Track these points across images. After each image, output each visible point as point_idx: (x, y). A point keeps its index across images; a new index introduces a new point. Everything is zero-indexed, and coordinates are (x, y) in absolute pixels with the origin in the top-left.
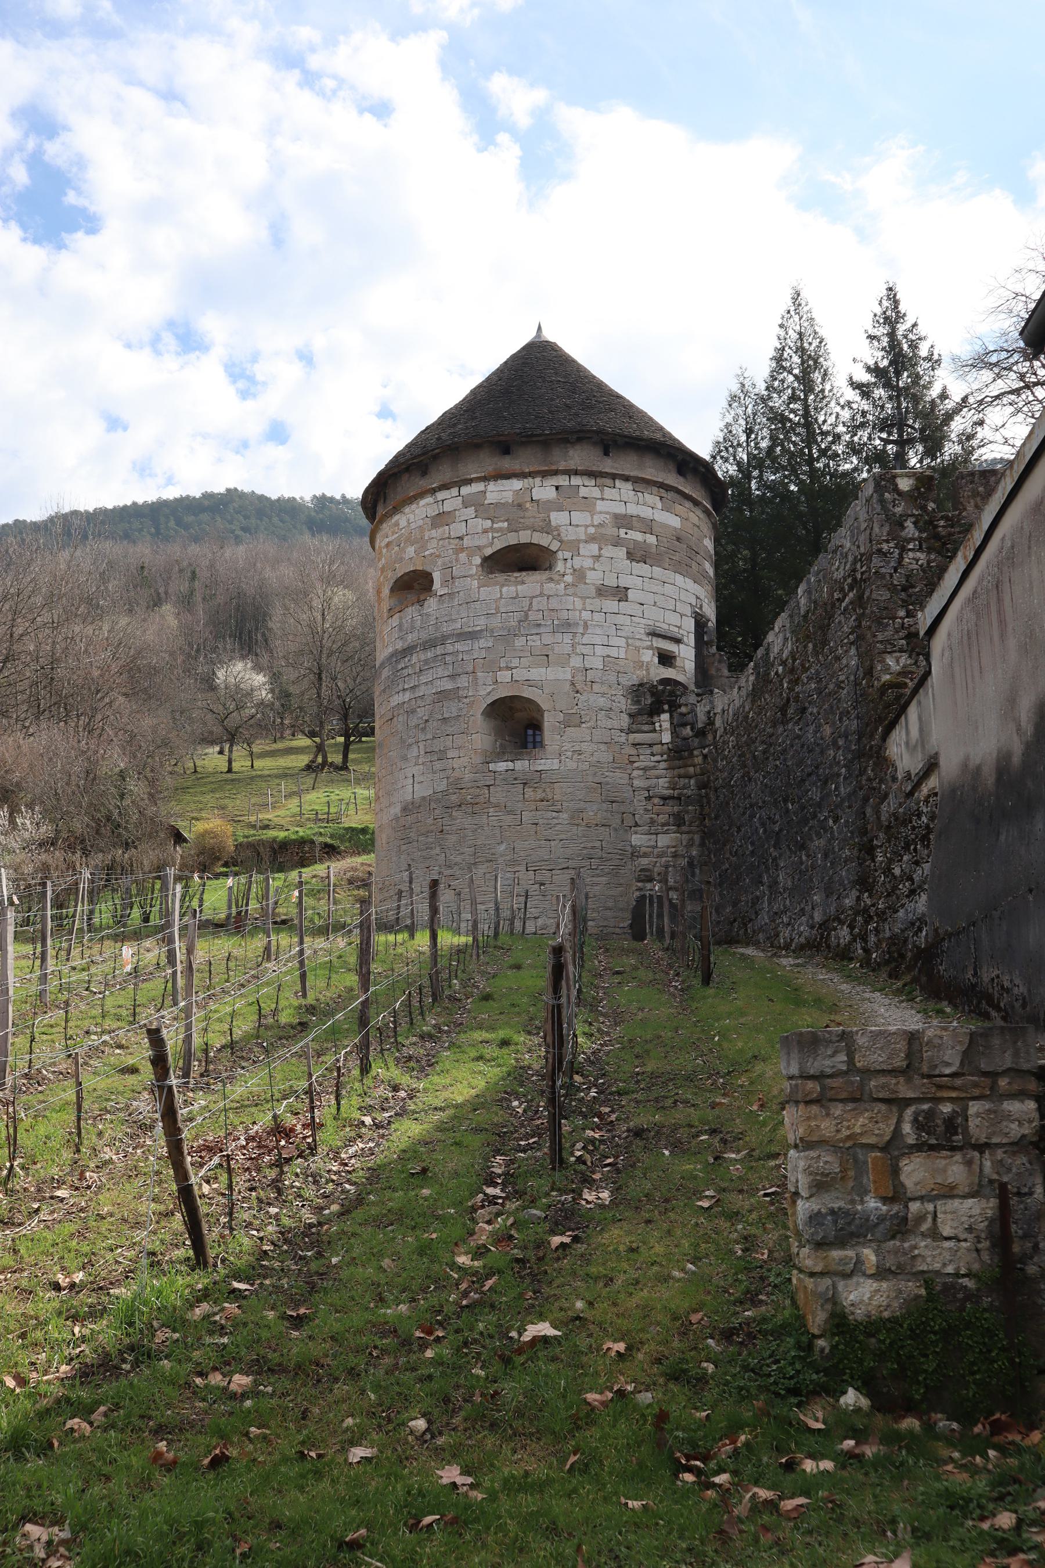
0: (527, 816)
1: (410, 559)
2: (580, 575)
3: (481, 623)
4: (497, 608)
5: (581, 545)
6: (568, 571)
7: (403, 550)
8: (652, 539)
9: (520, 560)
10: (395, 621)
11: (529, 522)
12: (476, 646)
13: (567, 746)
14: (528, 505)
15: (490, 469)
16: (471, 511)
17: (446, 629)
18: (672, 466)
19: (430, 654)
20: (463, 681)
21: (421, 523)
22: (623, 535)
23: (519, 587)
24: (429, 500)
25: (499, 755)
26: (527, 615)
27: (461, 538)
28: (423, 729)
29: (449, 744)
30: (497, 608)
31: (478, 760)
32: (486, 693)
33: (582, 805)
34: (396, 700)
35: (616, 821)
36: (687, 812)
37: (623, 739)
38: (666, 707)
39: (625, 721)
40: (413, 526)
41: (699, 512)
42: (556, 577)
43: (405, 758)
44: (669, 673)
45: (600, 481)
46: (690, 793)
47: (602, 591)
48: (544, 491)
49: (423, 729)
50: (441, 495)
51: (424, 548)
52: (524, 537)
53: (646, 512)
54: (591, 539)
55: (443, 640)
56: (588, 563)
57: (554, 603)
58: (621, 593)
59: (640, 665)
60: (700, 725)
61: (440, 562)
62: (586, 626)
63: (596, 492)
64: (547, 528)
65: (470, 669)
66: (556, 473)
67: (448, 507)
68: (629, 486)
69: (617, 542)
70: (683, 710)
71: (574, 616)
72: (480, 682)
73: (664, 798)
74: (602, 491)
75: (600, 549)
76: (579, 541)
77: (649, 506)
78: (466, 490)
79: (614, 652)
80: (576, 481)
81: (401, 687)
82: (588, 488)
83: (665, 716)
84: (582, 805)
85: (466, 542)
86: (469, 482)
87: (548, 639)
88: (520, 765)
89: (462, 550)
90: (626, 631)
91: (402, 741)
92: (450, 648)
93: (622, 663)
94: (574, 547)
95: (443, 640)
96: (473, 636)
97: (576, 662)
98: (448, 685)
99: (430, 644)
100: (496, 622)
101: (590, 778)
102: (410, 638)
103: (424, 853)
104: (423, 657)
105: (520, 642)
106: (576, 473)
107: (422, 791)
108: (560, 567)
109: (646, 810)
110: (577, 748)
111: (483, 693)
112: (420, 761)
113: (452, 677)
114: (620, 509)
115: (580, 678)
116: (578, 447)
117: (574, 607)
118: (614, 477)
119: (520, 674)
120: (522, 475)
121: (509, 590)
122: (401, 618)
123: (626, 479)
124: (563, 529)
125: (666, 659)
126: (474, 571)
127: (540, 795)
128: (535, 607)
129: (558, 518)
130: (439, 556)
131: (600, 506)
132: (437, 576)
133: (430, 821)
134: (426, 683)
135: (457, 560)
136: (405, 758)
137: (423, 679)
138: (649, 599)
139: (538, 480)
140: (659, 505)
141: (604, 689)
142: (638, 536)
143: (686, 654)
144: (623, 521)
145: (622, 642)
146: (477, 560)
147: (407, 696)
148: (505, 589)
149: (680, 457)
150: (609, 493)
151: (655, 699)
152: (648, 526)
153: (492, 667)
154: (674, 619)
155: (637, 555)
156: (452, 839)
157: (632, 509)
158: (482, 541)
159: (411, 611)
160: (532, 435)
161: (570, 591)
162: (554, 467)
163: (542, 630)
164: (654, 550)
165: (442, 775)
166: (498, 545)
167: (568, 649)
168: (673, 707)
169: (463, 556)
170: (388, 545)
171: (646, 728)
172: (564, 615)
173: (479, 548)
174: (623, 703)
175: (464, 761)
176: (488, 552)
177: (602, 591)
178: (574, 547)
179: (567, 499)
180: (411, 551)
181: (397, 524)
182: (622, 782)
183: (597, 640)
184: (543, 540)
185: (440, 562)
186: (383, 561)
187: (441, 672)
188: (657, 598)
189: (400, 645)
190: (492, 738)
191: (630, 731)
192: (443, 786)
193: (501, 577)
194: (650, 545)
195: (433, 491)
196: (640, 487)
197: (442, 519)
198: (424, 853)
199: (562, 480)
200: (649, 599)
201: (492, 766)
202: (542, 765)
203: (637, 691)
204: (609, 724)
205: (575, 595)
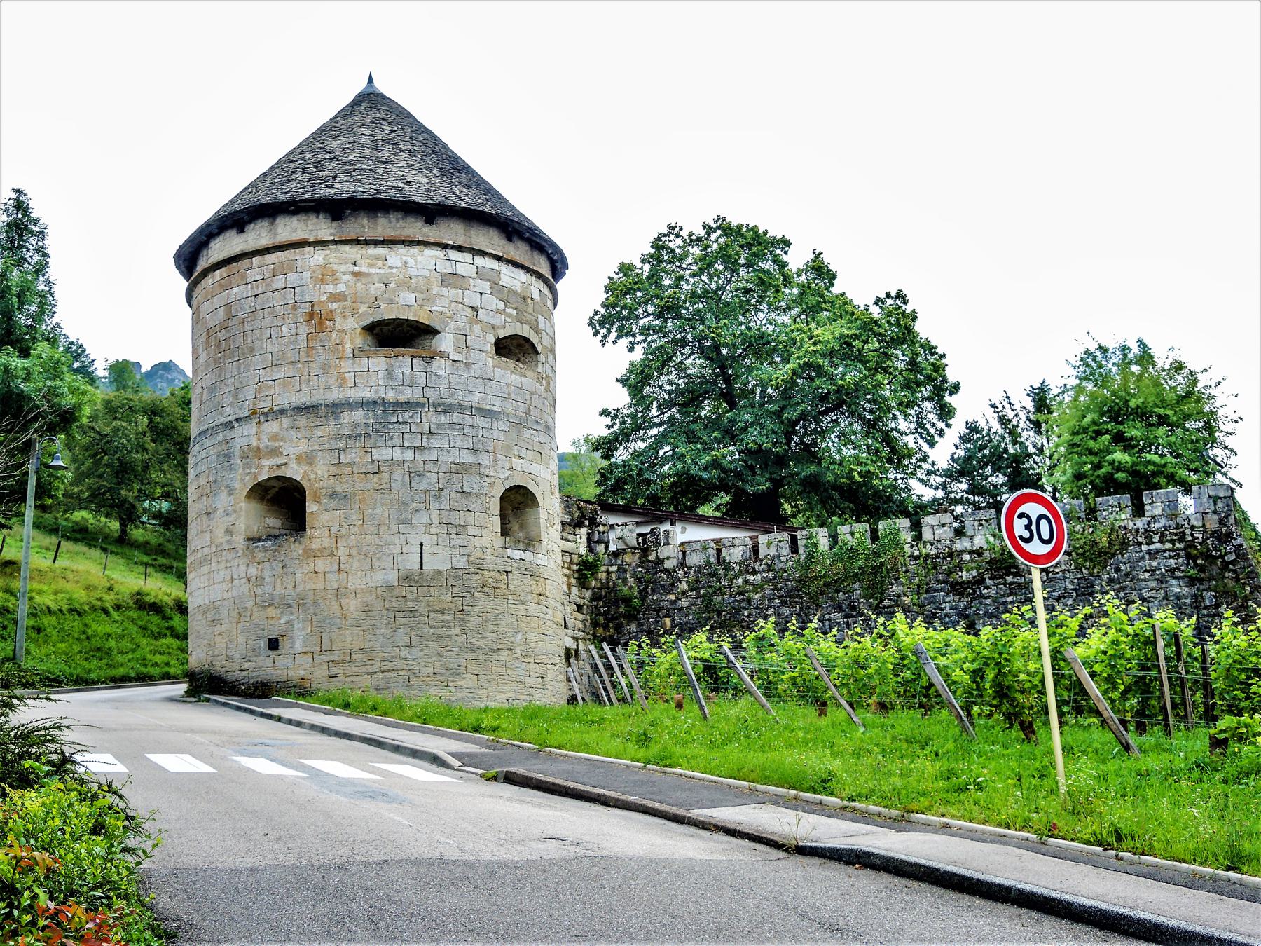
1: (405, 306)
3: (496, 405)
17: (460, 398)
19: (443, 419)
20: (484, 459)
21: (427, 273)
24: (438, 253)
28: (437, 498)
34: (385, 454)
38: (587, 522)
49: (437, 498)
50: (454, 255)
51: (433, 299)
55: (461, 409)
65: (491, 449)
67: (461, 269)
70: (601, 528)
72: (500, 465)
78: (479, 261)
86: (483, 254)
96: (491, 414)
98: (469, 459)
100: (509, 407)
103: (438, 632)
104: (434, 419)
112: (433, 530)
113: (474, 451)
133: (447, 598)
134: (442, 449)
136: (408, 522)
137: (435, 443)
147: (409, 455)
156: (475, 620)
158: (498, 320)
165: (463, 551)
169: (477, 328)
173: (494, 327)
176: (502, 334)
180: (409, 298)
184: (535, 340)
185: (452, 324)
187: (458, 441)
192: (463, 563)
195: (445, 247)
198: (438, 632)
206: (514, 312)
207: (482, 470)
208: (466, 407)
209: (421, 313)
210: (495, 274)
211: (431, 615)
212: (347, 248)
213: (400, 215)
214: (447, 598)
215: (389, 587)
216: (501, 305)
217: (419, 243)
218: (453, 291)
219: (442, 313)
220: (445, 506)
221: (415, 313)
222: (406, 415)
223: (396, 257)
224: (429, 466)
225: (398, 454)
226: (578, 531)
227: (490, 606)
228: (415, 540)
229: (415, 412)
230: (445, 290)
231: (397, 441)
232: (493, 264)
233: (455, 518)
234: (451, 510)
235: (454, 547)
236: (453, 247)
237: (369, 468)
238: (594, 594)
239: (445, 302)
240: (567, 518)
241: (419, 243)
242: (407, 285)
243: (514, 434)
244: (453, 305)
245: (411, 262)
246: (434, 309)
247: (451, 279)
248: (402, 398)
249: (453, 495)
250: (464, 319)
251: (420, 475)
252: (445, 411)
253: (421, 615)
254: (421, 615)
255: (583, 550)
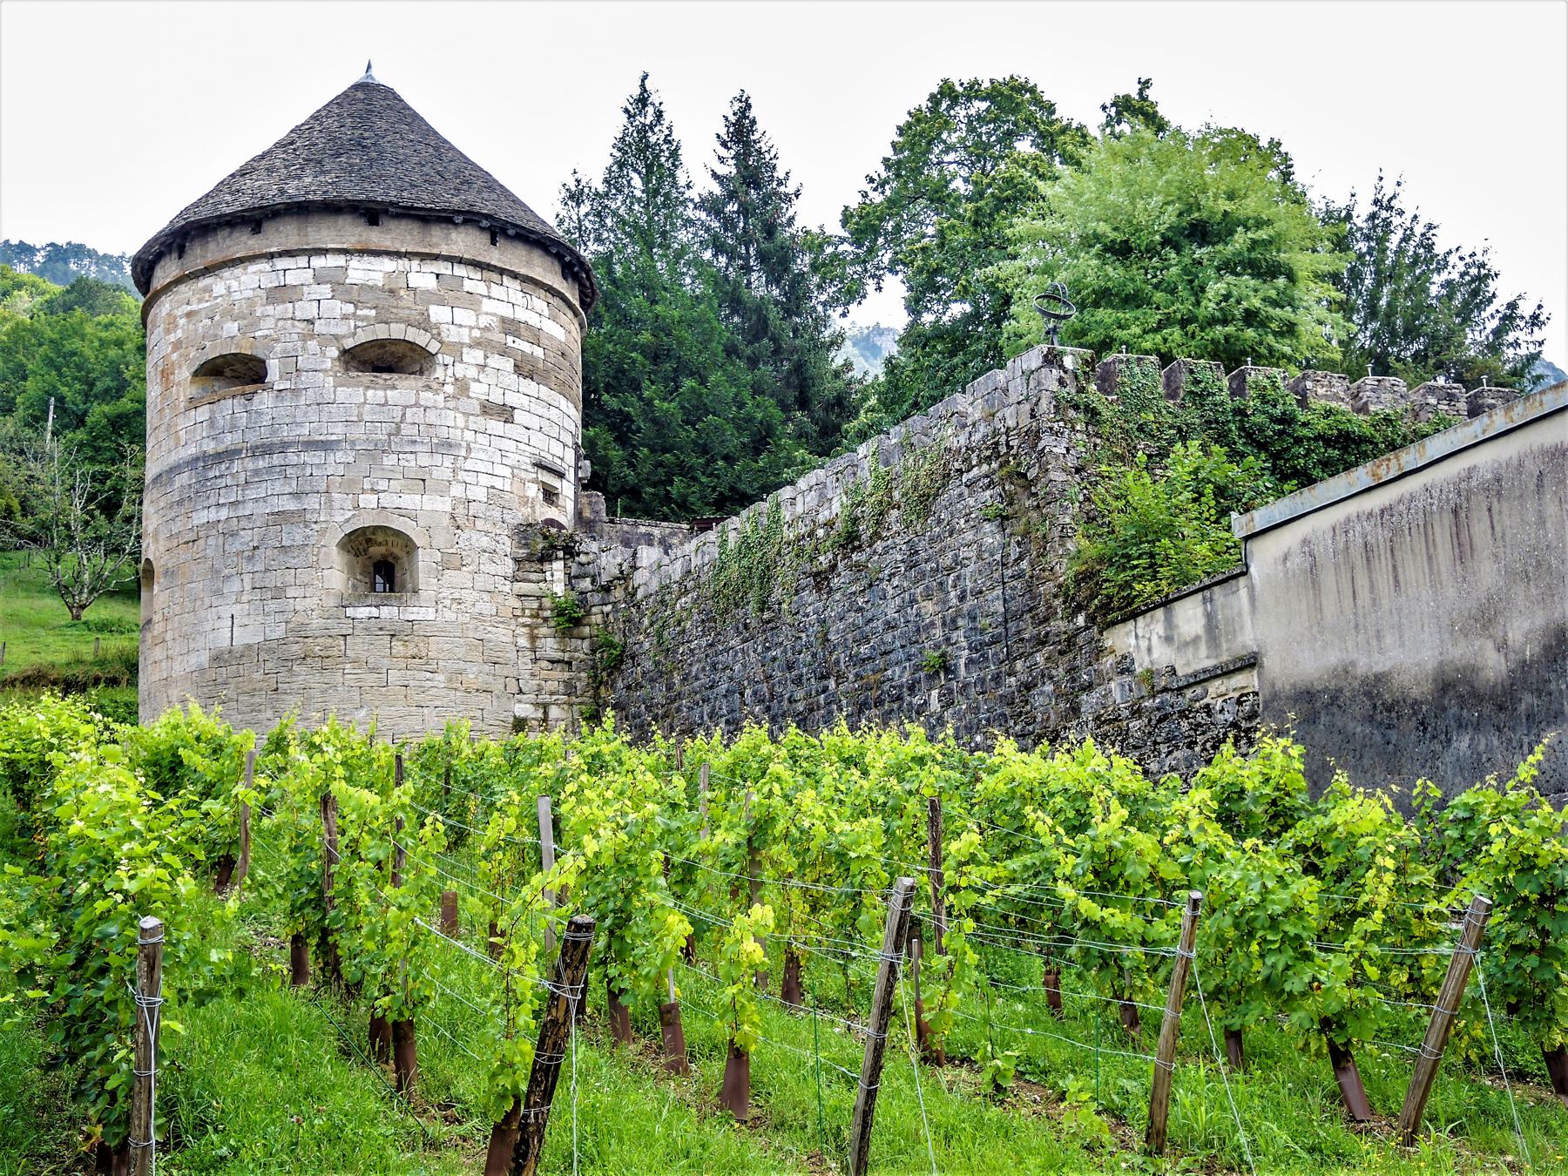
0: (394, 676)
1: (230, 338)
2: (462, 386)
3: (338, 432)
4: (360, 415)
5: (465, 350)
6: (449, 380)
7: (220, 326)
8: (539, 352)
9: (382, 359)
10: (203, 413)
11: (404, 313)
12: (331, 459)
13: (446, 593)
14: (402, 293)
15: (353, 240)
16: (326, 290)
17: (285, 434)
18: (558, 268)
19: (261, 464)
20: (312, 502)
21: (250, 294)
22: (510, 344)
23: (389, 393)
24: (264, 266)
25: (359, 601)
26: (399, 428)
27: (311, 322)
28: (250, 558)
29: (290, 579)
30: (360, 415)
31: (331, 602)
32: (342, 517)
33: (462, 665)
34: (201, 517)
35: (498, 687)
36: (579, 679)
37: (507, 589)
38: (561, 554)
39: (509, 567)
40: (237, 296)
41: (575, 321)
42: (434, 385)
43: (218, 593)
44: (552, 513)
45: (487, 274)
46: (582, 656)
47: (487, 409)
48: (422, 277)
49: (250, 558)
50: (281, 263)
51: (255, 324)
52: (397, 331)
53: (533, 320)
54: (476, 344)
55: (284, 447)
56: (472, 372)
57: (432, 417)
58: (506, 413)
59: (525, 501)
60: (604, 579)
61: (279, 347)
62: (469, 449)
63: (481, 288)
64: (425, 324)
65: (324, 488)
66: (437, 257)
67: (291, 279)
68: (516, 285)
69: (504, 352)
70: (583, 558)
71: (455, 435)
72: (336, 505)
73: (553, 662)
74: (489, 288)
75: (486, 357)
76: (462, 344)
77: (535, 311)
78: (318, 262)
79: (498, 483)
80: (460, 270)
81: (212, 501)
82: (474, 282)
83: (558, 565)
84: (462, 665)
85: (319, 327)
86: (324, 252)
87: (424, 460)
88: (385, 612)
89: (312, 337)
90: (512, 459)
91: (215, 572)
92: (292, 459)
93: (507, 497)
94: (456, 350)
95: (284, 447)
96: (326, 446)
97: (457, 490)
98: (291, 505)
99: (265, 450)
100: (357, 432)
101: (471, 634)
102: (229, 440)
103: (247, 717)
105: (391, 460)
106: (461, 261)
107: (242, 638)
108: (439, 373)
109: (533, 675)
110: (456, 596)
111: (340, 519)
112: (245, 598)
113: (296, 495)
114: (507, 312)
115: (461, 510)
116: (462, 229)
117: (453, 423)
118: (502, 271)
119: (388, 500)
120: (398, 255)
121: (375, 395)
122: (212, 412)
123: (515, 276)
124: (444, 328)
125: (550, 495)
126: (329, 364)
127: (412, 651)
128: (409, 418)
129: (438, 314)
130: (277, 340)
131: (487, 305)
132: (274, 367)
133: (258, 676)
134: (256, 500)
135: (304, 349)
136: (218, 593)
137: (251, 493)
138: (535, 423)
139: (415, 263)
140: (546, 312)
141: (488, 527)
142: (525, 347)
143: (567, 489)
144: (511, 327)
145: (507, 472)
146: (334, 352)
147: (224, 514)
148: (370, 393)
149: (568, 259)
150: (496, 290)
151: (542, 546)
152: (536, 336)
153: (352, 487)
154: (557, 449)
155: (526, 369)
157: (521, 315)
158: (342, 329)
160: (412, 208)
161: (451, 404)
162: (435, 251)
163: (418, 448)
164: (541, 366)
165: (279, 617)
166: (363, 337)
167: (448, 474)
168: (570, 552)
169: (312, 345)
170: (189, 315)
171: (533, 576)
172: (444, 432)
173: (336, 337)
174: (507, 545)
175: (312, 602)
176: (349, 343)
177: (487, 409)
178: (456, 350)
179: (450, 293)
180: (232, 328)
181: (208, 290)
182: (505, 639)
183: (481, 467)
184: (420, 338)
185: (279, 347)
186: (179, 334)
188: (545, 423)
189: (210, 447)
190: (344, 576)
191: (515, 580)
192: (279, 632)
193: (367, 377)
194: (537, 359)
195: (271, 256)
196: (529, 287)
197: (280, 294)
198: (247, 717)
199: (444, 268)
200: (535, 423)
201: (350, 612)
202: (413, 613)
203: (524, 532)
204: (492, 569)
205: (456, 409)
206: (373, 313)
207: (308, 516)
208: (290, 444)
209: (243, 343)
210: (340, 272)
211: (241, 698)
212: (182, 288)
213: (226, 232)
214: (258, 676)
215: (202, 670)
216: (350, 308)
217: (242, 260)
218: (280, 308)
219: (266, 337)
220: (260, 567)
221: (237, 345)
222: (223, 467)
223: (219, 285)
224: (244, 523)
225: (213, 515)
226: (547, 566)
227: (315, 680)
228: (226, 612)
229: (232, 461)
230: (270, 308)
231: (212, 501)
232: (340, 260)
233: (272, 580)
234: (267, 570)
235: (268, 614)
236: (281, 254)
237: (192, 536)
238: (592, 644)
239: (270, 323)
240: (522, 552)
241: (242, 260)
242: (229, 314)
243: (364, 466)
244: (281, 323)
245: (234, 285)
246: (257, 334)
247: (280, 294)
248: (221, 448)
249: (269, 552)
250: (295, 337)
251: (233, 534)
252: (264, 454)
253: (230, 700)
254: (230, 700)
255: (559, 589)
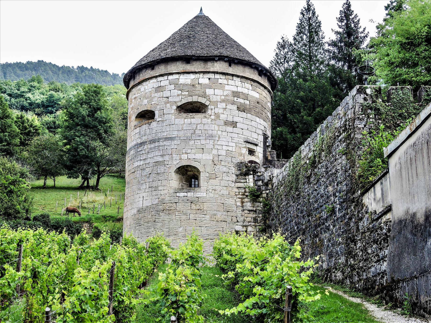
0: (192, 216)
1: (145, 106)
2: (217, 116)
3: (175, 133)
4: (182, 128)
5: (218, 104)
6: (213, 114)
7: (142, 101)
8: (247, 102)
9: (193, 108)
10: (137, 130)
11: (197, 93)
12: (173, 143)
13: (210, 187)
14: (197, 85)
15: (181, 69)
16: (172, 87)
17: (160, 135)
18: (256, 72)
19: (152, 146)
20: (167, 158)
21: (150, 90)
22: (236, 100)
23: (192, 120)
24: (154, 80)
25: (181, 190)
26: (195, 131)
27: (168, 98)
29: (160, 184)
30: (182, 128)
31: (172, 191)
32: (176, 163)
33: (215, 212)
34: (136, 164)
35: (229, 220)
36: (259, 217)
37: (233, 185)
38: (251, 173)
39: (234, 178)
40: (147, 91)
41: (266, 91)
42: (208, 116)
43: (139, 189)
44: (252, 158)
45: (227, 77)
46: (260, 209)
47: (226, 123)
48: (204, 80)
49: (148, 177)
50: (160, 79)
51: (151, 100)
52: (195, 99)
53: (245, 91)
54: (223, 101)
55: (159, 140)
56: (221, 111)
57: (206, 127)
58: (234, 124)
59: (241, 154)
60: (266, 181)
61: (158, 107)
62: (219, 137)
63: (225, 82)
64: (204, 96)
65: (170, 153)
66: (209, 72)
67: (162, 84)
68: (239, 79)
69: (233, 103)
71: (214, 133)
72: (174, 159)
73: (249, 211)
74: (228, 81)
75: (226, 105)
76: (217, 102)
77: (246, 88)
78: (170, 77)
79: (230, 149)
80: (217, 76)
81: (139, 159)
82: (222, 80)
83: (251, 177)
84: (215, 212)
85: (170, 99)
87: (203, 142)
88: (189, 194)
89: (168, 102)
90: (236, 140)
91: (139, 182)
92: (161, 144)
93: (234, 153)
94: (216, 104)
95: (159, 140)
97: (215, 152)
98: (160, 159)
99: (153, 141)
100: (181, 133)
101: (219, 201)
102: (144, 139)
103: (146, 230)
104: (149, 147)
105: (192, 142)
106: (218, 73)
107: (147, 203)
108: (209, 112)
109: (242, 215)
110: (214, 188)
111: (175, 163)
113: (162, 156)
114: (235, 89)
115: (216, 159)
116: (218, 62)
117: (214, 129)
118: (233, 75)
119: (191, 156)
120: (196, 73)
121: (187, 121)
122: (140, 130)
123: (238, 76)
124: (211, 96)
125: (251, 152)
126: (173, 112)
127: (198, 207)
128: (198, 128)
129: (209, 92)
130: (158, 105)
131: (227, 87)
132: (157, 113)
133: (150, 217)
134: (151, 158)
135: (166, 107)
136: (139, 189)
137: (149, 156)
138: (245, 127)
139: (201, 75)
140: (251, 88)
141: (226, 164)
142: (242, 101)
143: (259, 151)
144: (236, 94)
145: (234, 145)
146: (175, 107)
147: (142, 163)
148: (186, 120)
149: (260, 69)
150: (230, 82)
151: (246, 170)
152: (246, 97)
153: (179, 153)
154: (255, 136)
155: (241, 109)
156: (159, 224)
157: (240, 90)
158: (177, 99)
159: (145, 127)
160: (200, 56)
161: (213, 122)
162: (208, 70)
163: (201, 138)
164: (248, 107)
165: (156, 197)
166: (184, 102)
167: (212, 147)
168: (255, 172)
169: (168, 105)
170: (135, 98)
171: (242, 181)
172: (210, 132)
173: (175, 102)
174: (234, 170)
175: (166, 192)
176: (179, 104)
177: (226, 123)
178: (216, 104)
179: (213, 84)
180: (145, 101)
181: (139, 90)
182: (232, 203)
183: (224, 143)
186: (133, 105)
187: (157, 153)
188: (249, 127)
189: (139, 141)
190: (178, 182)
191: (236, 182)
192: (156, 202)
193: (185, 115)
194: (246, 105)
195: (156, 77)
196: (243, 80)
197: (159, 89)
198: (146, 230)
199: (211, 76)
200: (245, 127)
201: (178, 194)
202: (198, 194)
203: (240, 165)
204: (227, 178)
205: (215, 124)
206: (187, 93)
207: (165, 163)
209: (148, 106)
210: (177, 80)
212: (134, 90)
218: (159, 94)
219: (155, 104)
220: (151, 180)
222: (142, 147)
224: (147, 166)
226: (247, 177)
227: (166, 218)
232: (176, 76)
233: (154, 184)
240: (238, 172)
243: (183, 145)
244: (159, 99)
245: (146, 87)
249: (154, 175)
250: (163, 103)
253: (142, 225)
254: (142, 225)
255: (252, 185)
